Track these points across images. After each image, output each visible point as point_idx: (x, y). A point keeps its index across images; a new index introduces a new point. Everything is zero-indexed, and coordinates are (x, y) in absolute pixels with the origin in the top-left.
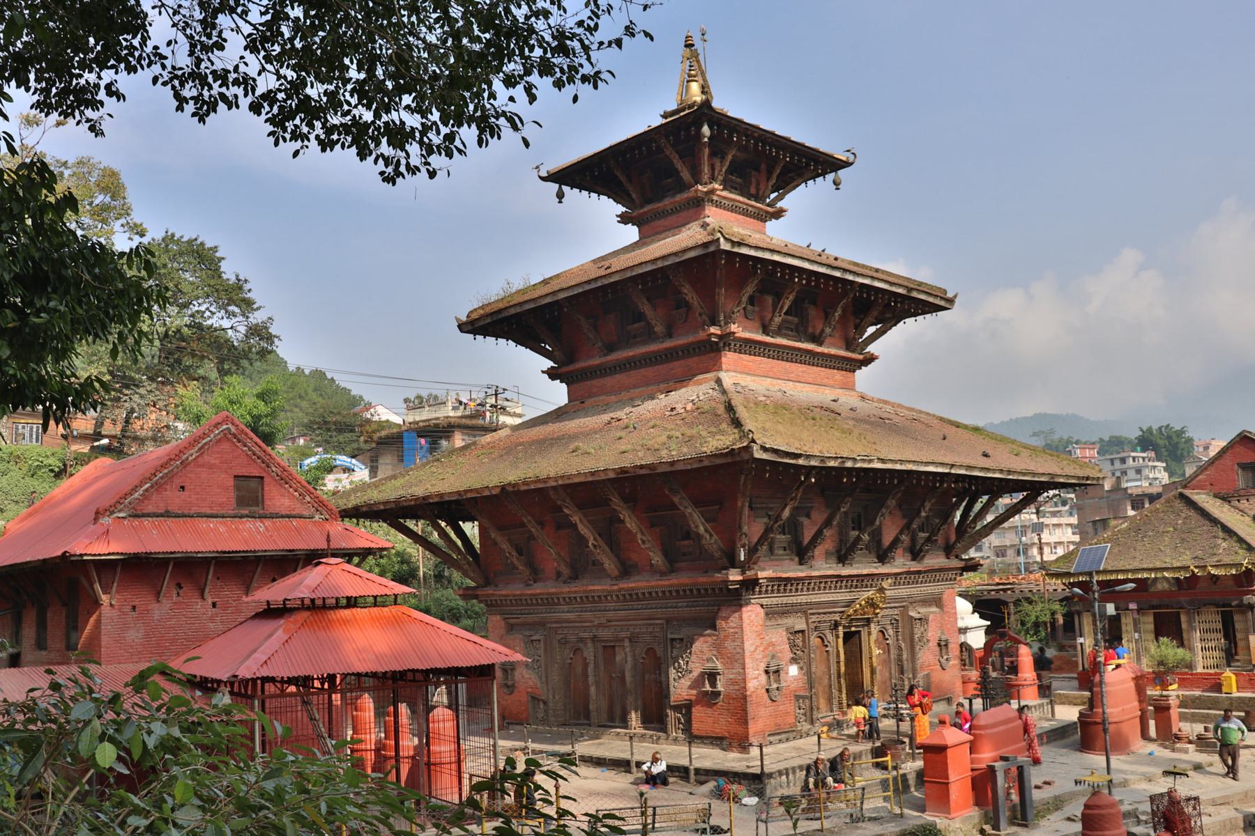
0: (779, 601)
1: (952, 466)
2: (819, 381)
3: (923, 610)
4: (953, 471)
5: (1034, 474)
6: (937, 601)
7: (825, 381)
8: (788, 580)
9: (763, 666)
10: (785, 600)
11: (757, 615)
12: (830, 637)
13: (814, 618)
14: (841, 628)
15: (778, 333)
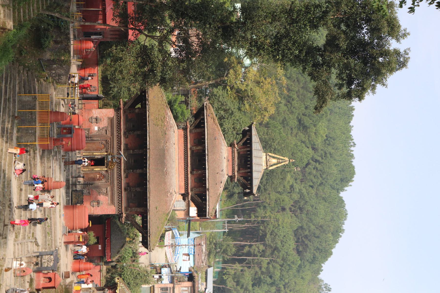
0: (115, 124)
1: (149, 149)
2: (180, 174)
3: (109, 193)
4: (148, 150)
5: (149, 198)
6: (112, 202)
7: (180, 178)
8: (120, 124)
9: (98, 116)
10: (115, 126)
11: (111, 114)
12: (104, 150)
13: (110, 141)
14: (106, 153)
15: (192, 152)
